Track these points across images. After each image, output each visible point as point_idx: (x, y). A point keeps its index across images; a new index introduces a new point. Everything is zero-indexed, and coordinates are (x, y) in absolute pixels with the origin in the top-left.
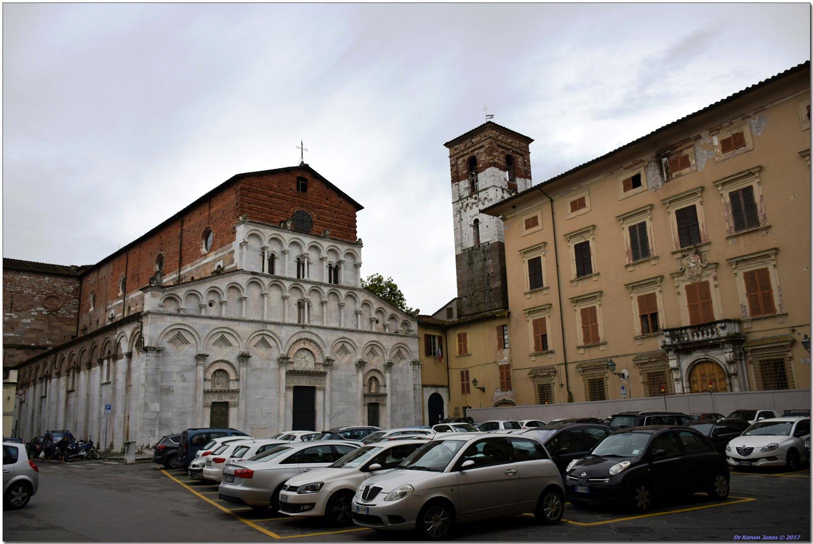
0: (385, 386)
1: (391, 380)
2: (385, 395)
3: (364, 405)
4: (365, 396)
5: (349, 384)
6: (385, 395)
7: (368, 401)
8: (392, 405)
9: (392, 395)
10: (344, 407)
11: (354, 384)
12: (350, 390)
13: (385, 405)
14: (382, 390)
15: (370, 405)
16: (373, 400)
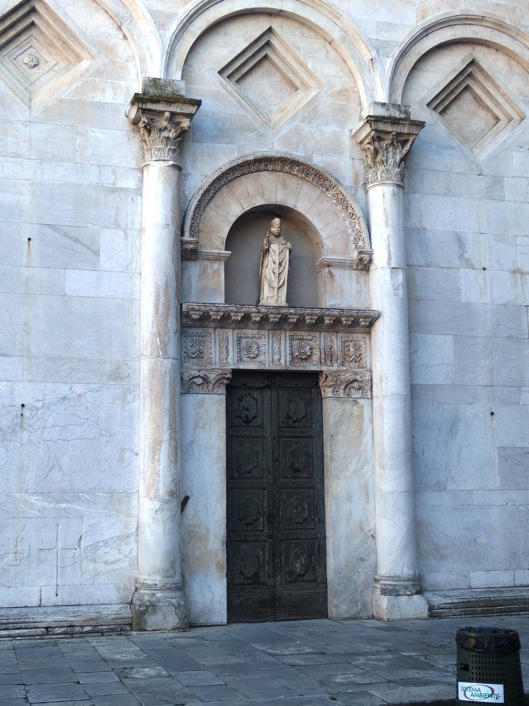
0: (364, 265)
1: (410, 234)
2: (363, 322)
3: (185, 385)
4: (189, 323)
5: (74, 244)
6: (363, 322)
7: (225, 353)
8: (414, 394)
9: (413, 326)
10: (26, 393)
11: (109, 240)
12: (77, 282)
13: (359, 386)
14: (340, 293)
15: (240, 385)
16: (273, 353)
